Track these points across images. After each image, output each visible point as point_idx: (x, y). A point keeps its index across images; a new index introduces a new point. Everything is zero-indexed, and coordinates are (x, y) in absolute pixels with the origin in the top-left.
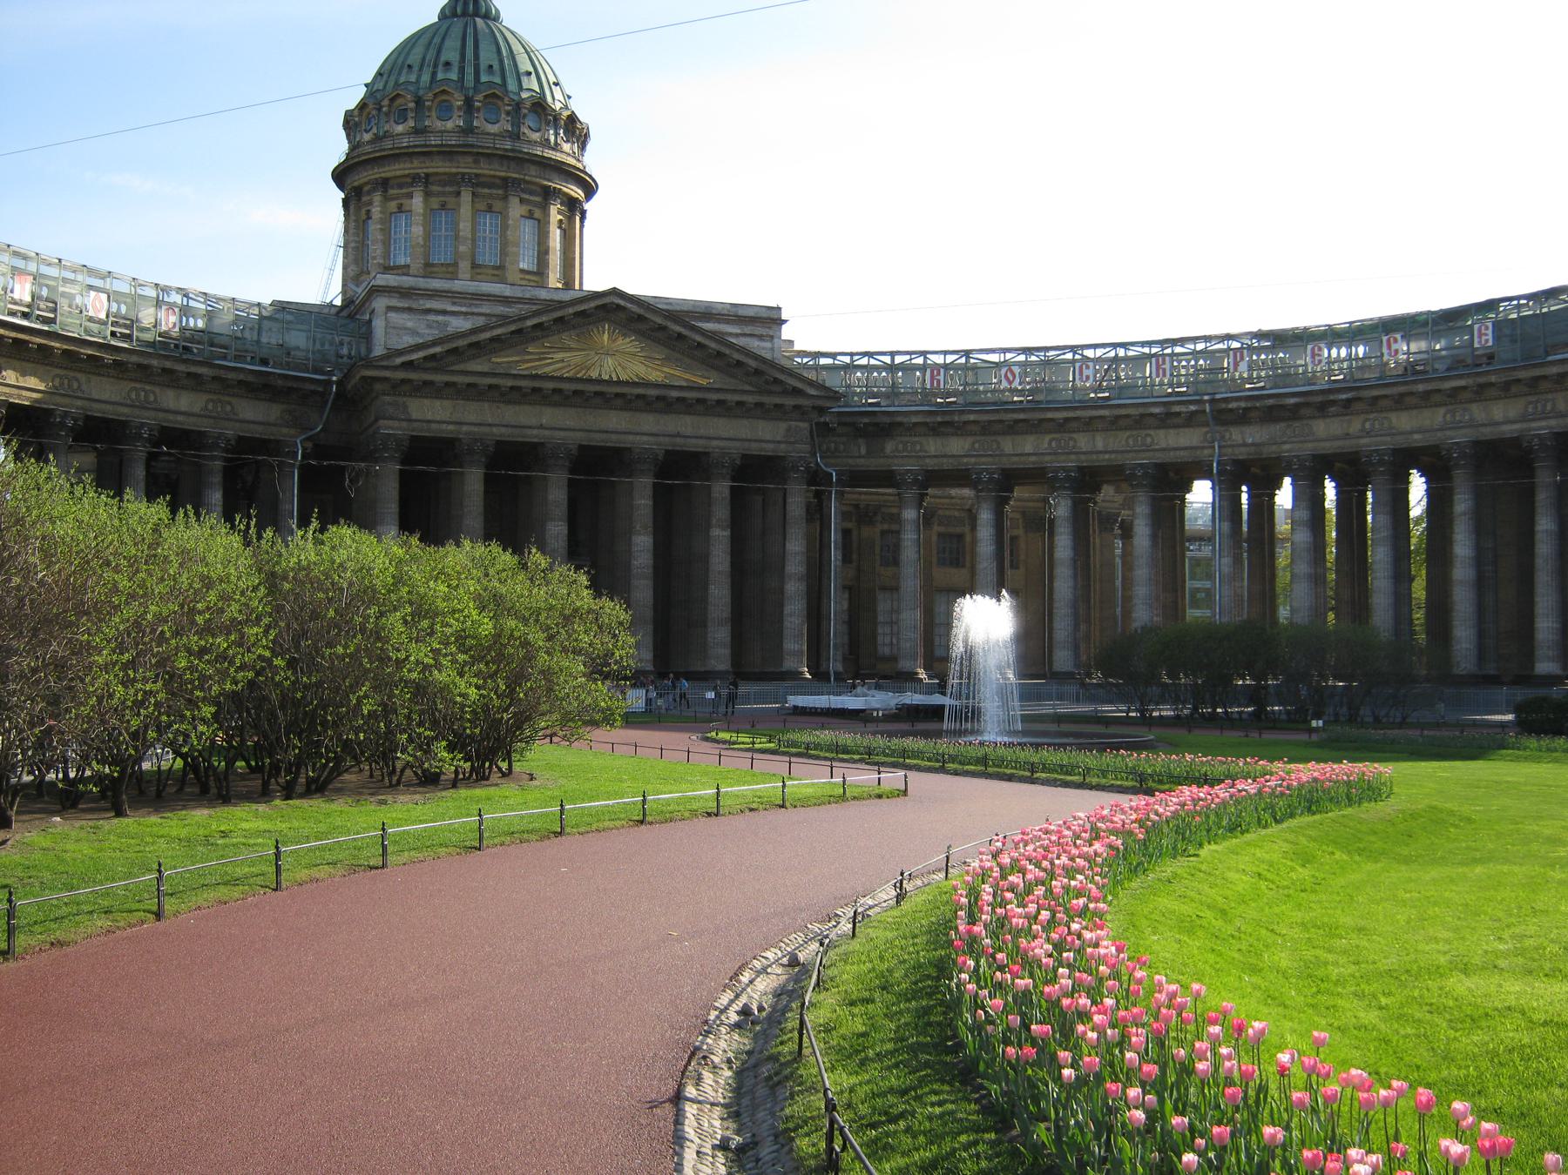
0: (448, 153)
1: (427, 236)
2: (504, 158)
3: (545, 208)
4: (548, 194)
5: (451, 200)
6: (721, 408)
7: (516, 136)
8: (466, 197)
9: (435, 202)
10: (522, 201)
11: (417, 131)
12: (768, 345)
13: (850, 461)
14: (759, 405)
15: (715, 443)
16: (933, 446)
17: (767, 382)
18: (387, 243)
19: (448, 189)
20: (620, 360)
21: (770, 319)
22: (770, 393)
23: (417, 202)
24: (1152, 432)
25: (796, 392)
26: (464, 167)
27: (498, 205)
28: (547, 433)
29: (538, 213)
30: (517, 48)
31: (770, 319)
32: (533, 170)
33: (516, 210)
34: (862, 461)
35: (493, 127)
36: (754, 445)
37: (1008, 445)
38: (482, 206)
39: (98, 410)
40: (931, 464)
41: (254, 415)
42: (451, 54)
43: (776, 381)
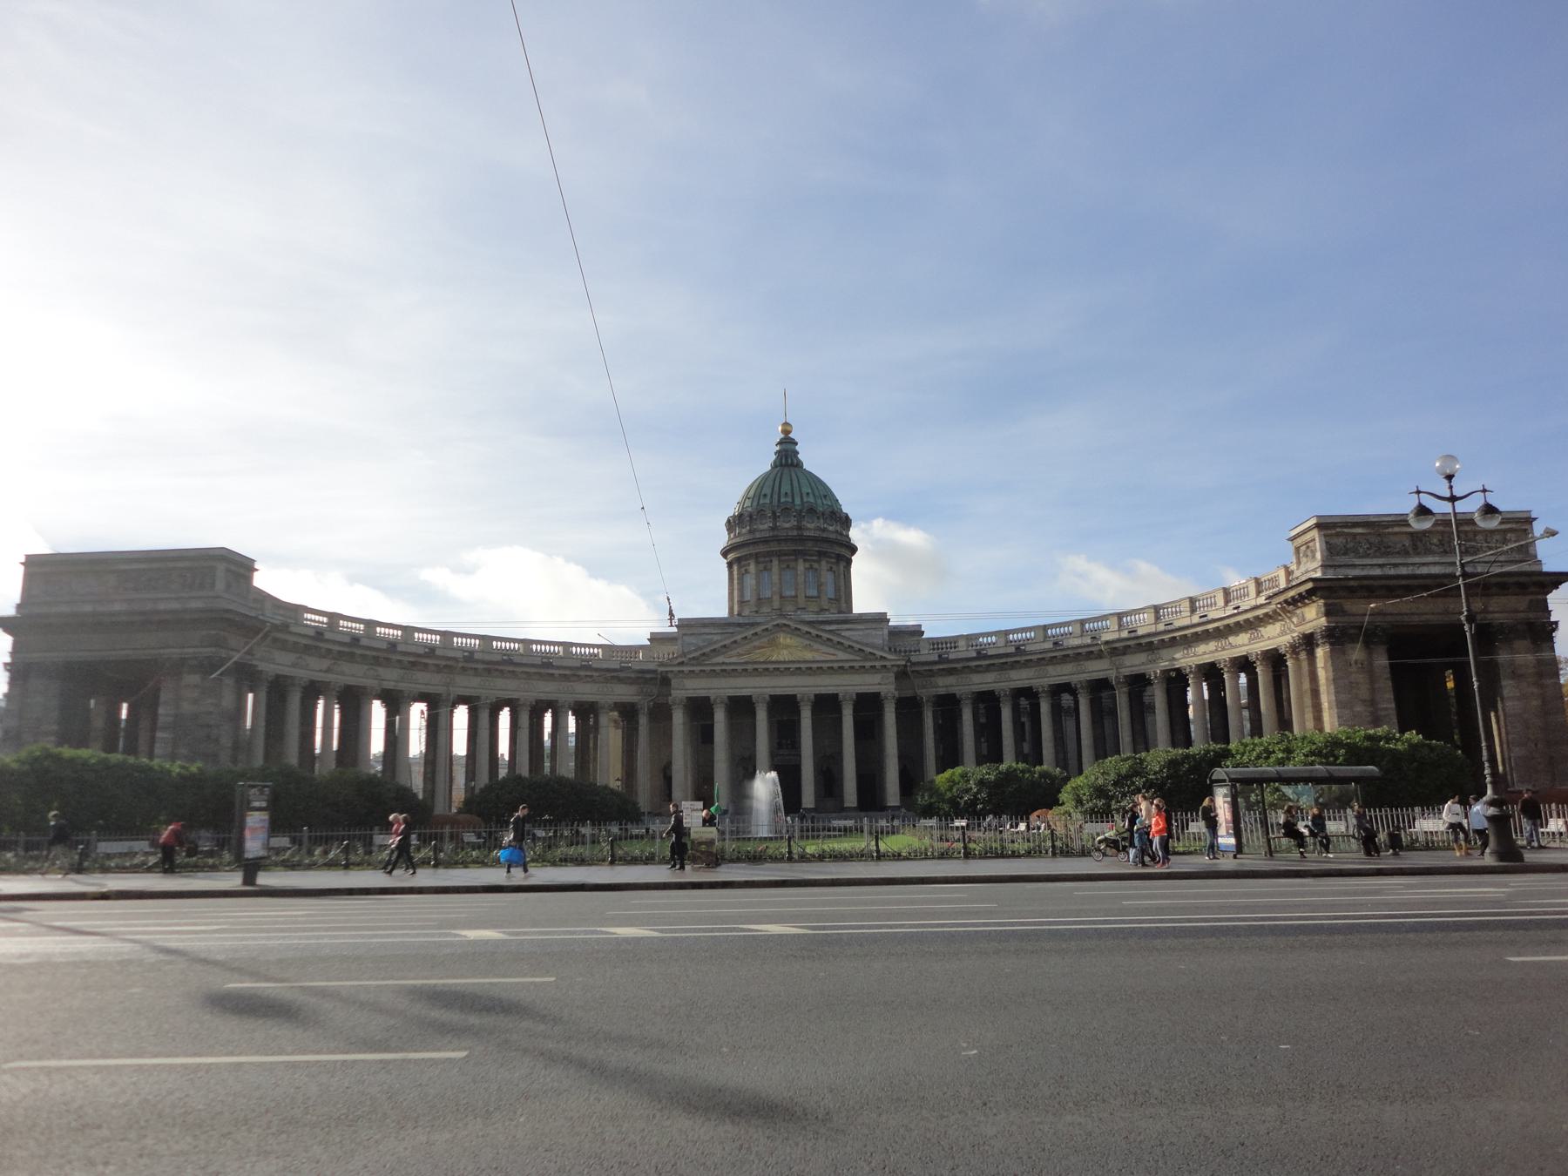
0: (765, 541)
1: (758, 583)
2: (793, 540)
3: (819, 562)
4: (822, 554)
7: (799, 528)
8: (775, 562)
9: (761, 566)
11: (750, 532)
16: (976, 678)
18: (741, 590)
20: (789, 649)
22: (866, 660)
23: (752, 568)
26: (774, 547)
27: (792, 564)
29: (816, 565)
30: (804, 481)
32: (810, 544)
33: (801, 566)
35: (787, 524)
37: (1014, 674)
39: (543, 697)
41: (625, 693)
42: (767, 491)
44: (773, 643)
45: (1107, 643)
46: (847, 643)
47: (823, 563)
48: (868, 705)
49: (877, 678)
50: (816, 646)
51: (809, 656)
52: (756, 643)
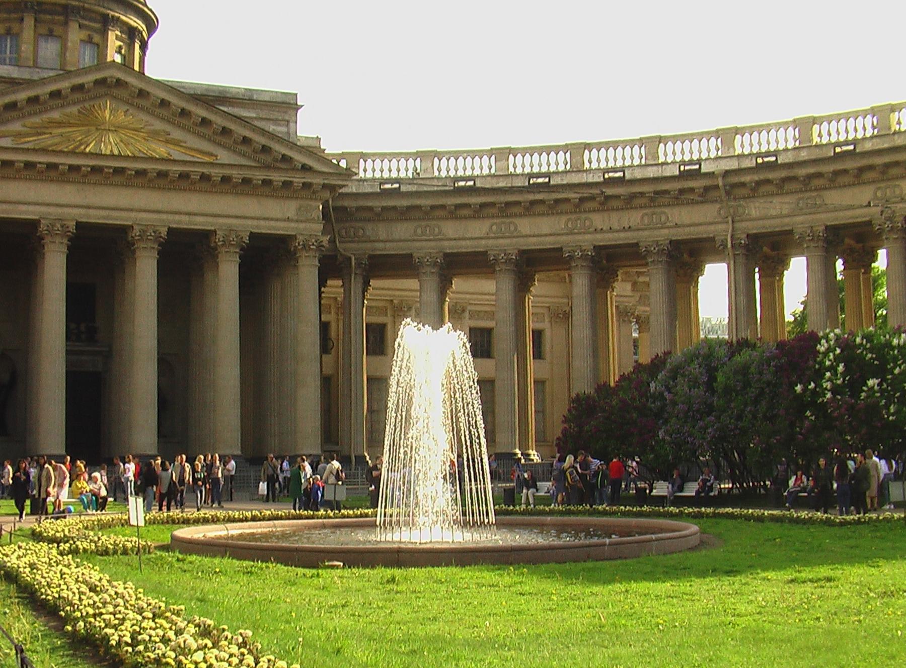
3: (104, 34)
4: (107, 22)
5: (15, 27)
6: (227, 184)
8: (29, 21)
10: (81, 26)
12: (283, 129)
13: (369, 245)
14: (267, 183)
15: (221, 220)
16: (450, 229)
17: (276, 160)
19: (13, 16)
21: (286, 106)
24: (666, 210)
25: (305, 168)
27: (58, 30)
28: (43, 209)
29: (97, 38)
31: (286, 106)
33: (75, 35)
34: (381, 245)
36: (262, 223)
37: (525, 225)
38: (43, 30)
40: (450, 247)
43: (285, 159)
44: (89, 121)
45: (727, 173)
46: (241, 131)
47: (111, 36)
48: (265, 259)
49: (290, 208)
50: (177, 134)
51: (161, 150)
52: (56, 115)
